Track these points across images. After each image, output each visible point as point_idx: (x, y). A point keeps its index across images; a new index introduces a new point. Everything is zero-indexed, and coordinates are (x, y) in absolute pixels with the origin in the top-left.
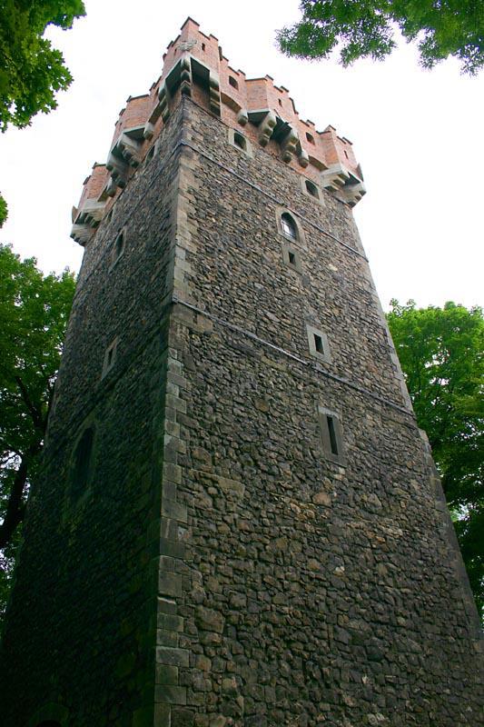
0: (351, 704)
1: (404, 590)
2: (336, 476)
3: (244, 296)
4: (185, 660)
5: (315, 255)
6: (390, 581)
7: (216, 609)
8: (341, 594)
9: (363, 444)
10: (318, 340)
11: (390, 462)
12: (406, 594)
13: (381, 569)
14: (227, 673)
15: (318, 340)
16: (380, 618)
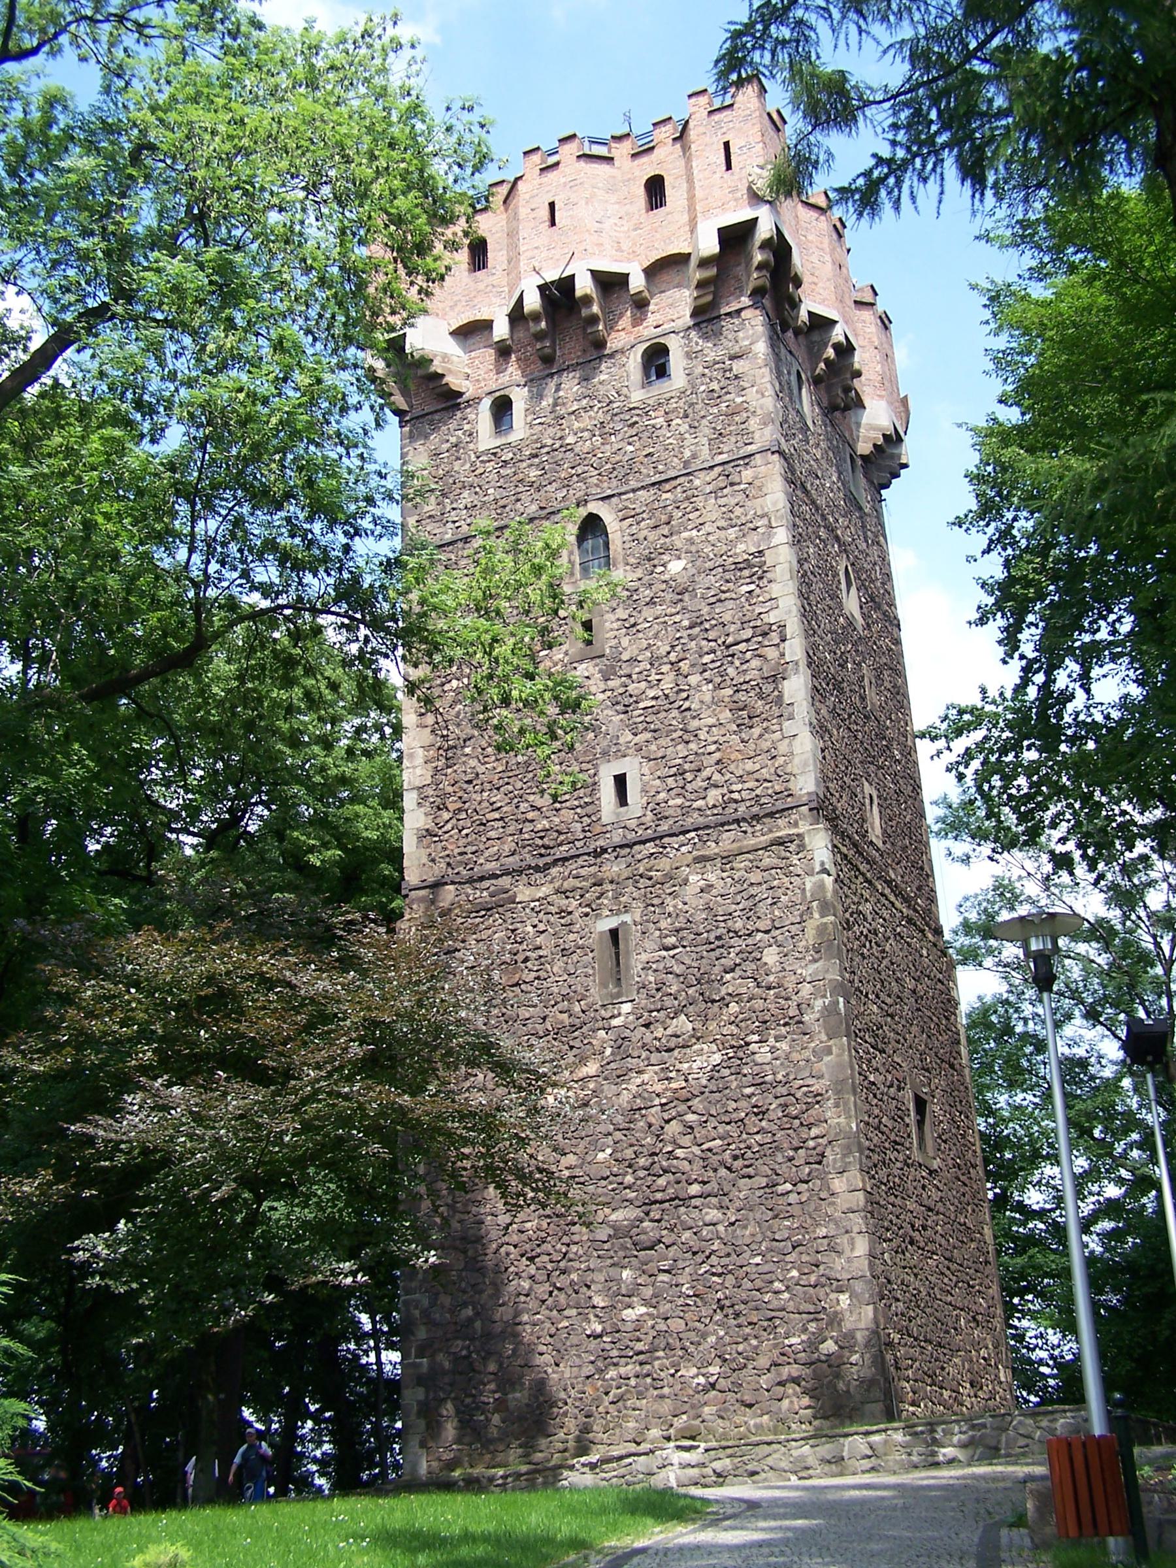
0: (602, 1304)
1: (704, 1147)
2: (615, 1022)
3: (497, 797)
4: (425, 1302)
5: (639, 573)
6: (686, 1141)
7: (455, 1248)
8: (603, 1183)
9: (672, 940)
10: (620, 781)
11: (718, 944)
12: (710, 1150)
13: (674, 1128)
14: (465, 1305)
15: (620, 781)
16: (659, 1196)
